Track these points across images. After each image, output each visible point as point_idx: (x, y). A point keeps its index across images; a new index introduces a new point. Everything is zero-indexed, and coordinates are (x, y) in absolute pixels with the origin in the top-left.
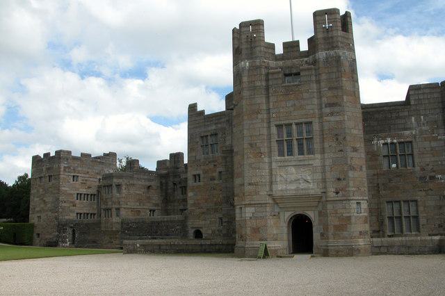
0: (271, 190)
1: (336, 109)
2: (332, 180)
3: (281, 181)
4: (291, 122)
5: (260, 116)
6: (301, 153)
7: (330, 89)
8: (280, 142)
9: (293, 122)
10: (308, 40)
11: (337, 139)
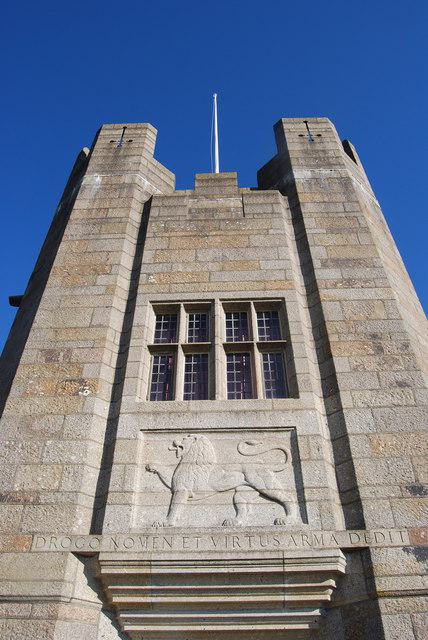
0: (96, 528)
1: (359, 273)
2: (383, 491)
3: (147, 491)
4: (210, 296)
5: (102, 280)
6: (242, 386)
7: (331, 231)
8: (163, 353)
9: (217, 297)
10: (259, 173)
11: (380, 350)
